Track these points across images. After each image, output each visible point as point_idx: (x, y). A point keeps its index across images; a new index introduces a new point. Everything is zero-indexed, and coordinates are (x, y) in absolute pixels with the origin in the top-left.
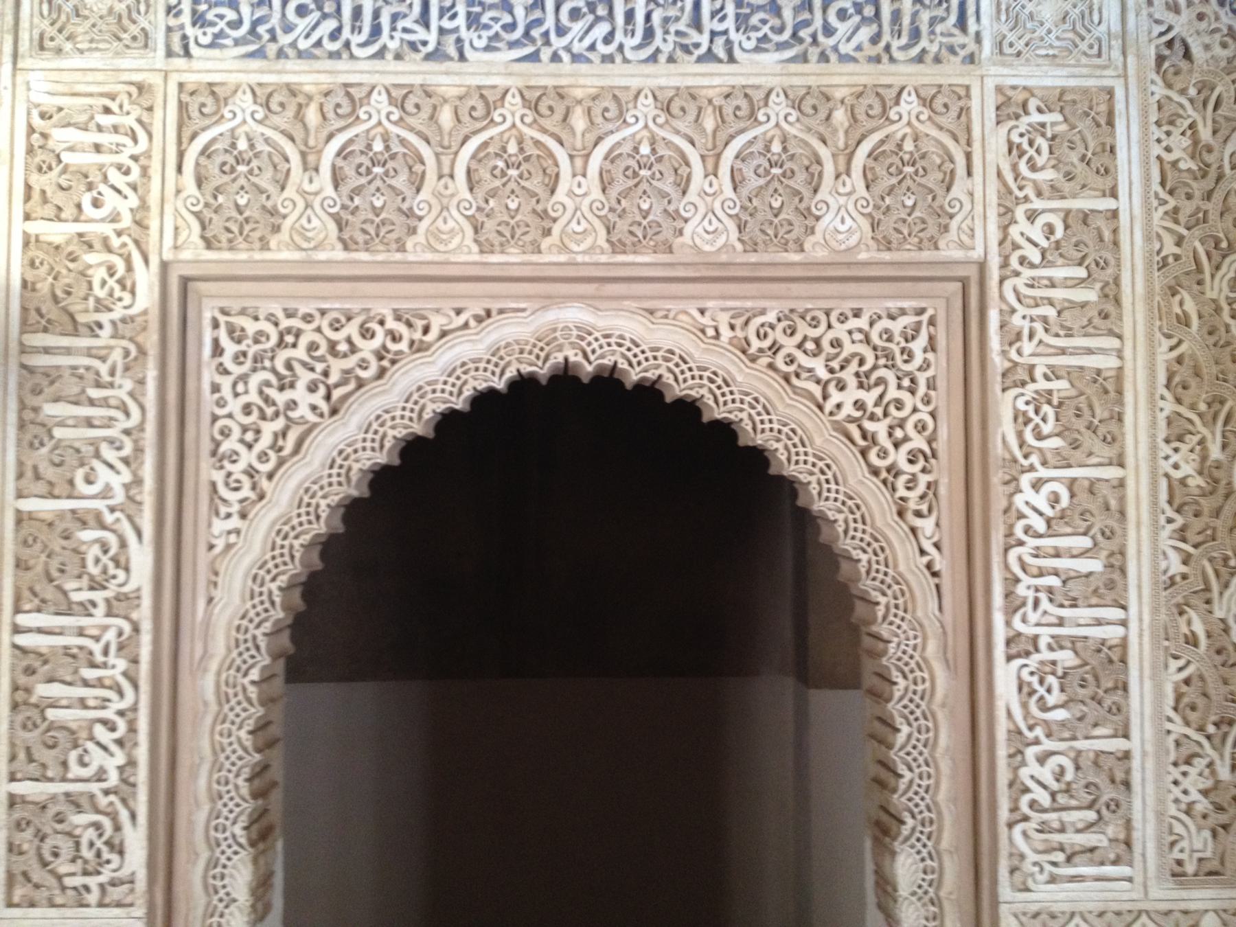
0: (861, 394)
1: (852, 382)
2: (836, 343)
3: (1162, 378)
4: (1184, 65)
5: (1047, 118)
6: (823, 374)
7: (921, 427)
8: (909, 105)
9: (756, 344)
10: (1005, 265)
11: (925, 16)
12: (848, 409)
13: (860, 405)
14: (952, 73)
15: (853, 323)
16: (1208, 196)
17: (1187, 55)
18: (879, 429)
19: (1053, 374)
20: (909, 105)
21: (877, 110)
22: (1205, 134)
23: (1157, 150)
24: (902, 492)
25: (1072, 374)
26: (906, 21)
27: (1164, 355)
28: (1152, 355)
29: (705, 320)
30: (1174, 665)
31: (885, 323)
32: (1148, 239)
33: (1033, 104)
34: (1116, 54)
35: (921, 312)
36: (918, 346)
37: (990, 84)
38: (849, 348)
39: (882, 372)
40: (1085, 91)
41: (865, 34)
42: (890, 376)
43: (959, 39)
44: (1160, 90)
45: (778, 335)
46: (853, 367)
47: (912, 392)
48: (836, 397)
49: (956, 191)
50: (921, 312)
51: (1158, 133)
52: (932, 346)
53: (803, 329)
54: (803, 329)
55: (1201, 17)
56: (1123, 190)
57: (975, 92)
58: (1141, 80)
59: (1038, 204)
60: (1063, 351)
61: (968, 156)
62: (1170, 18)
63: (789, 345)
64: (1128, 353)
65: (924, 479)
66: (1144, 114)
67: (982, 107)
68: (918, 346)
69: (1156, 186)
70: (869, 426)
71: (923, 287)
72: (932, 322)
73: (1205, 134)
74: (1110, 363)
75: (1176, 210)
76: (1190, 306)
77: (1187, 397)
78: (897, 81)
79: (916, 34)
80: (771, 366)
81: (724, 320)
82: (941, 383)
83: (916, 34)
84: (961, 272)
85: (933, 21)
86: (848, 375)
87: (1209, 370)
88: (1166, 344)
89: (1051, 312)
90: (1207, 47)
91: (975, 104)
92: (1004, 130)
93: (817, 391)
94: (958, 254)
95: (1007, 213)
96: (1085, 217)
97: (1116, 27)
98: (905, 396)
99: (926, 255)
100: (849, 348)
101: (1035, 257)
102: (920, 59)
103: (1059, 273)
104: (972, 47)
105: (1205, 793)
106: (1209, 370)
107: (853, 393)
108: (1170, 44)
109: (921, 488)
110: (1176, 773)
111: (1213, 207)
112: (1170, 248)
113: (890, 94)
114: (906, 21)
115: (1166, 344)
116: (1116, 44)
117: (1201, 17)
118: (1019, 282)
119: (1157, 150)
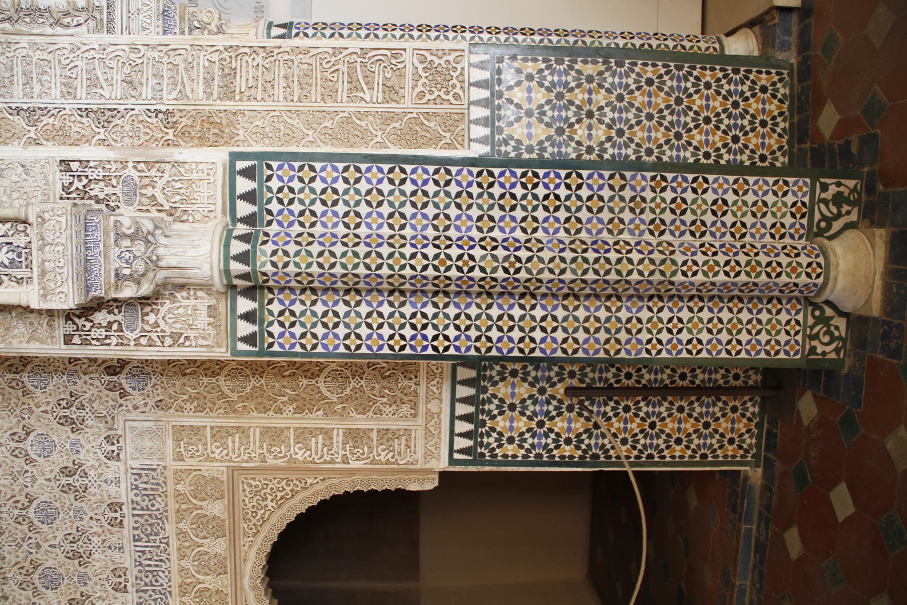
0: (269, 500)
1: (265, 503)
2: (253, 507)
3: (262, 415)
4: (164, 402)
5: (182, 445)
6: (262, 511)
7: (279, 483)
8: (180, 487)
9: (254, 530)
10: (229, 461)
11: (152, 481)
12: (274, 504)
13: (272, 501)
14: (169, 474)
15: (247, 502)
16: (205, 397)
17: (161, 401)
18: (279, 495)
19: (261, 447)
20: (180, 487)
21: (181, 497)
22: (185, 397)
23: (191, 413)
24: (299, 489)
25: (261, 442)
26: (154, 487)
27: (255, 414)
28: (255, 418)
29: (247, 545)
30: (351, 414)
31: (247, 493)
32: (219, 418)
33: (178, 450)
34: (161, 423)
35: (243, 482)
36: (254, 483)
37: (173, 463)
38: (255, 504)
39: (262, 494)
40: (173, 434)
41: (159, 499)
42: (263, 491)
43: (159, 471)
44: (172, 411)
45: (251, 524)
46: (260, 502)
47: (268, 485)
48: (270, 508)
49: (206, 475)
50: (243, 482)
51: (186, 412)
52: (254, 479)
53: (249, 516)
54: (249, 516)
55: (148, 396)
56: (205, 424)
57: (175, 467)
58: (169, 417)
59: (209, 450)
60: (254, 443)
61: (195, 470)
62: (149, 406)
63: (254, 521)
64: (255, 425)
65: (295, 482)
66: (180, 416)
67: (180, 466)
68: (254, 483)
69: (203, 414)
70: (278, 498)
71: (235, 481)
72: (246, 479)
73: (185, 397)
74: (258, 430)
75: (210, 408)
76: (240, 405)
77: (268, 407)
78: (173, 491)
79: (158, 484)
80: (261, 525)
81: (246, 539)
82: (265, 476)
83: (158, 484)
84: (230, 472)
85: (153, 479)
86: (263, 504)
87: (260, 400)
88: (252, 413)
89: (243, 448)
90: (158, 395)
91: (179, 468)
92: (187, 459)
93: (268, 513)
94: (225, 475)
95: (213, 460)
96: (213, 436)
97: (153, 423)
98: (269, 487)
99: (226, 484)
100: (255, 504)
101: (225, 452)
102: (165, 483)
103: (230, 444)
104: (161, 467)
105: (390, 405)
106: (260, 400)
107: (268, 502)
108: (158, 406)
109: (297, 483)
110: (384, 415)
111: (209, 396)
112: (222, 411)
113: (177, 493)
114: (154, 487)
115: (252, 413)
116: (158, 423)
117: (148, 396)
118: (233, 456)
119: (191, 413)
